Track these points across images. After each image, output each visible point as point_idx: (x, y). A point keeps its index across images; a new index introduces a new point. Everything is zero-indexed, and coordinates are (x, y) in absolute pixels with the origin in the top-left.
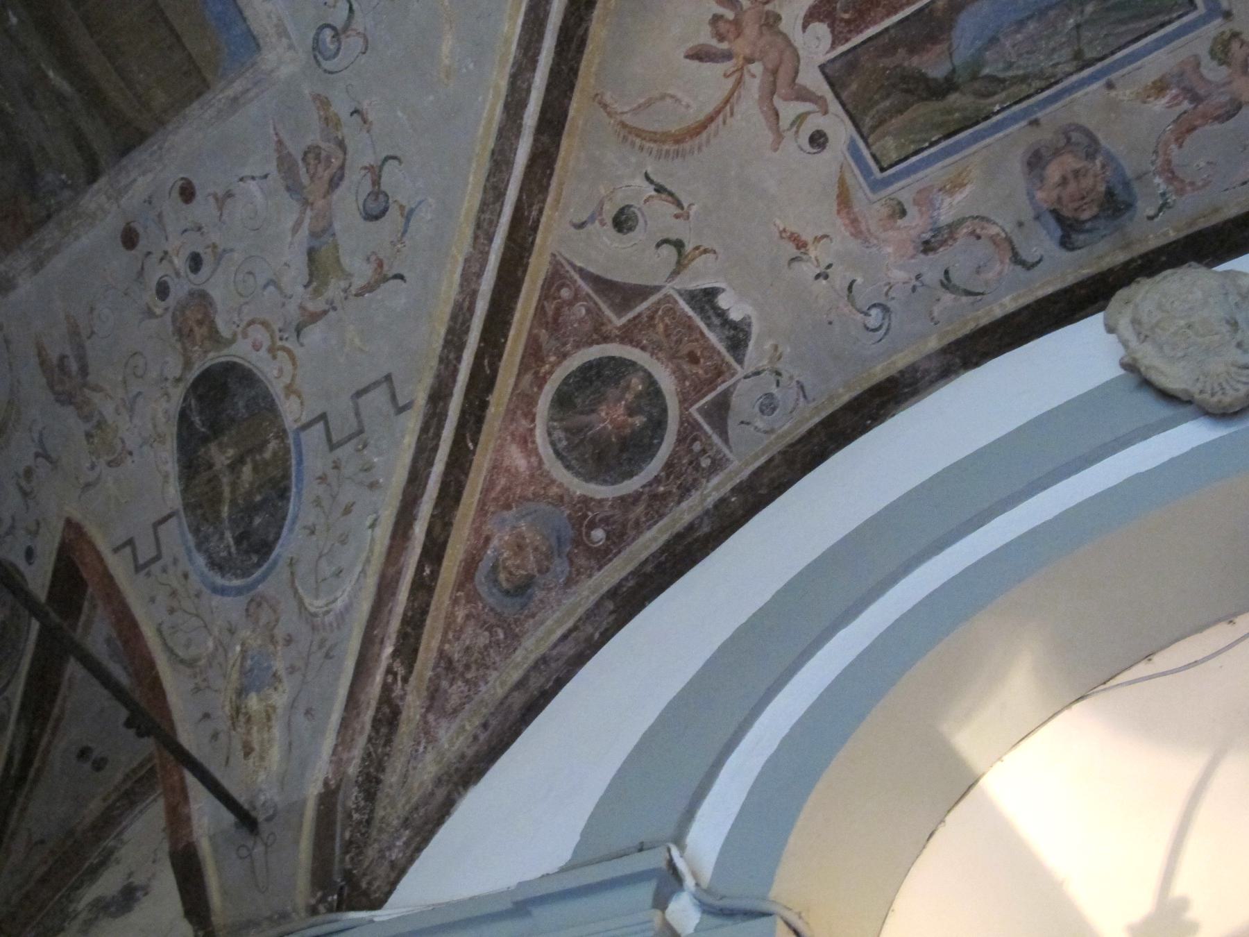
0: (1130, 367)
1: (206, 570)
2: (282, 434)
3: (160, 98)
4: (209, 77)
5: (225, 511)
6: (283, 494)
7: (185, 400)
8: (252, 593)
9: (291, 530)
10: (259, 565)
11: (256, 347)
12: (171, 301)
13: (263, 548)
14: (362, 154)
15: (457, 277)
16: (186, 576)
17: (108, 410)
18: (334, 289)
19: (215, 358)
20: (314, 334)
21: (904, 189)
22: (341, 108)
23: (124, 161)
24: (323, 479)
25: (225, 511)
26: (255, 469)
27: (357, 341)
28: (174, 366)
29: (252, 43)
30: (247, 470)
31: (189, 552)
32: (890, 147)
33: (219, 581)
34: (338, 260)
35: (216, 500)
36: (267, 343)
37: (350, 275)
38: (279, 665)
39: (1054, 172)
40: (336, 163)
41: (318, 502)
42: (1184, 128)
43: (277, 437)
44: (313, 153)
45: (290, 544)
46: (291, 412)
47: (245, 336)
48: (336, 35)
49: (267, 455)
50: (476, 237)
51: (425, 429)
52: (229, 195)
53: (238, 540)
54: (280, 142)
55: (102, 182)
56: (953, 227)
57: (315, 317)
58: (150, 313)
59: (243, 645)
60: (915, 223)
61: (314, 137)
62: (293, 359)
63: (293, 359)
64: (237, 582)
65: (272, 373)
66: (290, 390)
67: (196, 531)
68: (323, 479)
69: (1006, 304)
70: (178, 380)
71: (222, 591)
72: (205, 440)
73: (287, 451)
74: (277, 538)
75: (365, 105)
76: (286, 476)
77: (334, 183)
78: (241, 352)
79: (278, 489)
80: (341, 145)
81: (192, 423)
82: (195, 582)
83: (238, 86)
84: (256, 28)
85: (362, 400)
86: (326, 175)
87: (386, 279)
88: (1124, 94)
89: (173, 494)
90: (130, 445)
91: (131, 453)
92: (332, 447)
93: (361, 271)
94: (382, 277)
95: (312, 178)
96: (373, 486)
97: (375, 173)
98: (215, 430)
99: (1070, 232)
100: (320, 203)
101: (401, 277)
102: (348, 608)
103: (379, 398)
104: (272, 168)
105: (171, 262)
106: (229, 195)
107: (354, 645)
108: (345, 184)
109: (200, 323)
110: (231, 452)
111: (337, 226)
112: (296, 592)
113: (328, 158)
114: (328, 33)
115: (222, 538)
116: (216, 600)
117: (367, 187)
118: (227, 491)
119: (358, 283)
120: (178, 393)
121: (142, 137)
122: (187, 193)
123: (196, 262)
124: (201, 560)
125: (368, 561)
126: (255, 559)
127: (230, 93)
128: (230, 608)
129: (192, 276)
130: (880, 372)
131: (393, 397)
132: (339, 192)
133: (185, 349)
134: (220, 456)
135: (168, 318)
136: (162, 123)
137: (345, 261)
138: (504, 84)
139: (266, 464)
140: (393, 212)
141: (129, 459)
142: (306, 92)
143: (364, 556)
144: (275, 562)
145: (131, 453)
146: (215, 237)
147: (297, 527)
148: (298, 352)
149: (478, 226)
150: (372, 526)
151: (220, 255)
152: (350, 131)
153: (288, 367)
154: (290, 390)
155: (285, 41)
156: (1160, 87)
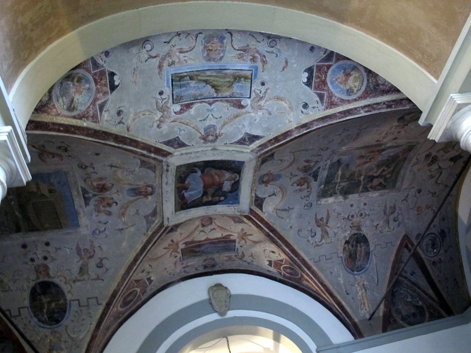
0: (210, 299)
1: (38, 322)
2: (66, 300)
3: (47, 225)
4: (64, 227)
5: (45, 311)
6: (65, 312)
7: (35, 285)
8: (53, 330)
9: (66, 319)
10: (55, 324)
11: (61, 281)
12: (35, 263)
13: (58, 321)
14: (99, 254)
15: (116, 284)
16: (30, 322)
17: (6, 280)
18: (86, 277)
19: (46, 279)
20: (78, 284)
21: (184, 262)
22: (96, 244)
23: (30, 233)
24: (77, 312)
25: (45, 311)
26: (56, 305)
27: (90, 289)
28: (33, 277)
29: (78, 226)
30: (53, 305)
31: (31, 317)
32: (185, 257)
33: (42, 325)
34: (88, 272)
35: (42, 308)
36: (64, 280)
37: (90, 276)
38: (63, 346)
39: (207, 262)
40: (92, 254)
41: (75, 316)
42: (227, 261)
43: (64, 300)
44: (86, 250)
45: (65, 322)
46: (69, 297)
47: (58, 277)
48: (100, 232)
49: (60, 303)
50: (122, 279)
51: (105, 309)
52: (60, 249)
53: (49, 318)
54: (78, 244)
55: (20, 234)
56: (189, 266)
57: (79, 280)
58: (27, 264)
59: (50, 340)
60: (184, 265)
61: (88, 247)
62: (71, 286)
63: (71, 286)
64: (49, 326)
65: (65, 288)
66: (69, 292)
67: (34, 313)
68: (77, 312)
69: (192, 274)
70: (33, 281)
71: (43, 327)
72: (40, 294)
73: (66, 303)
74: (62, 320)
75: (102, 246)
76: (66, 308)
77: (91, 257)
78: (56, 281)
79: (63, 311)
80: (94, 251)
81: (36, 291)
82: (33, 323)
83: (70, 231)
84: (80, 224)
85: (89, 300)
86: (89, 255)
87: (99, 279)
88: (221, 256)
89: (27, 303)
90: (11, 288)
91: (12, 291)
92: (80, 306)
93: (93, 276)
94: (98, 278)
95: (85, 254)
96: (91, 317)
97: (101, 260)
98: (44, 293)
99: (205, 267)
100: (86, 260)
101: (103, 280)
102: (83, 339)
103: (94, 301)
104: (74, 248)
105: (37, 255)
106: (60, 249)
107: (85, 346)
108: (93, 259)
109: (44, 271)
110: (48, 299)
111: (89, 266)
112: (67, 332)
113: (90, 253)
114: (97, 231)
115: (43, 316)
116: (41, 329)
117: (99, 261)
118: (46, 307)
119: (92, 278)
120: (32, 284)
121: (38, 230)
122: (47, 244)
123: (45, 258)
124: (36, 320)
125: (89, 331)
126: (54, 323)
127: (68, 231)
128: (47, 332)
129: (43, 260)
130: (168, 282)
131: (97, 302)
132: (90, 260)
133: (37, 274)
134: (45, 299)
135: (33, 267)
136: (46, 229)
137: (90, 273)
138: (134, 255)
139: (59, 304)
140: (104, 268)
141: (11, 292)
142: (88, 238)
143: (87, 330)
144: (61, 325)
145: (12, 291)
146: (53, 255)
147: (68, 319)
148: (73, 285)
149: (123, 277)
150: (90, 324)
151: (53, 259)
152: (97, 250)
153: (70, 288)
154: (69, 292)
155: (86, 228)
156: (226, 257)
